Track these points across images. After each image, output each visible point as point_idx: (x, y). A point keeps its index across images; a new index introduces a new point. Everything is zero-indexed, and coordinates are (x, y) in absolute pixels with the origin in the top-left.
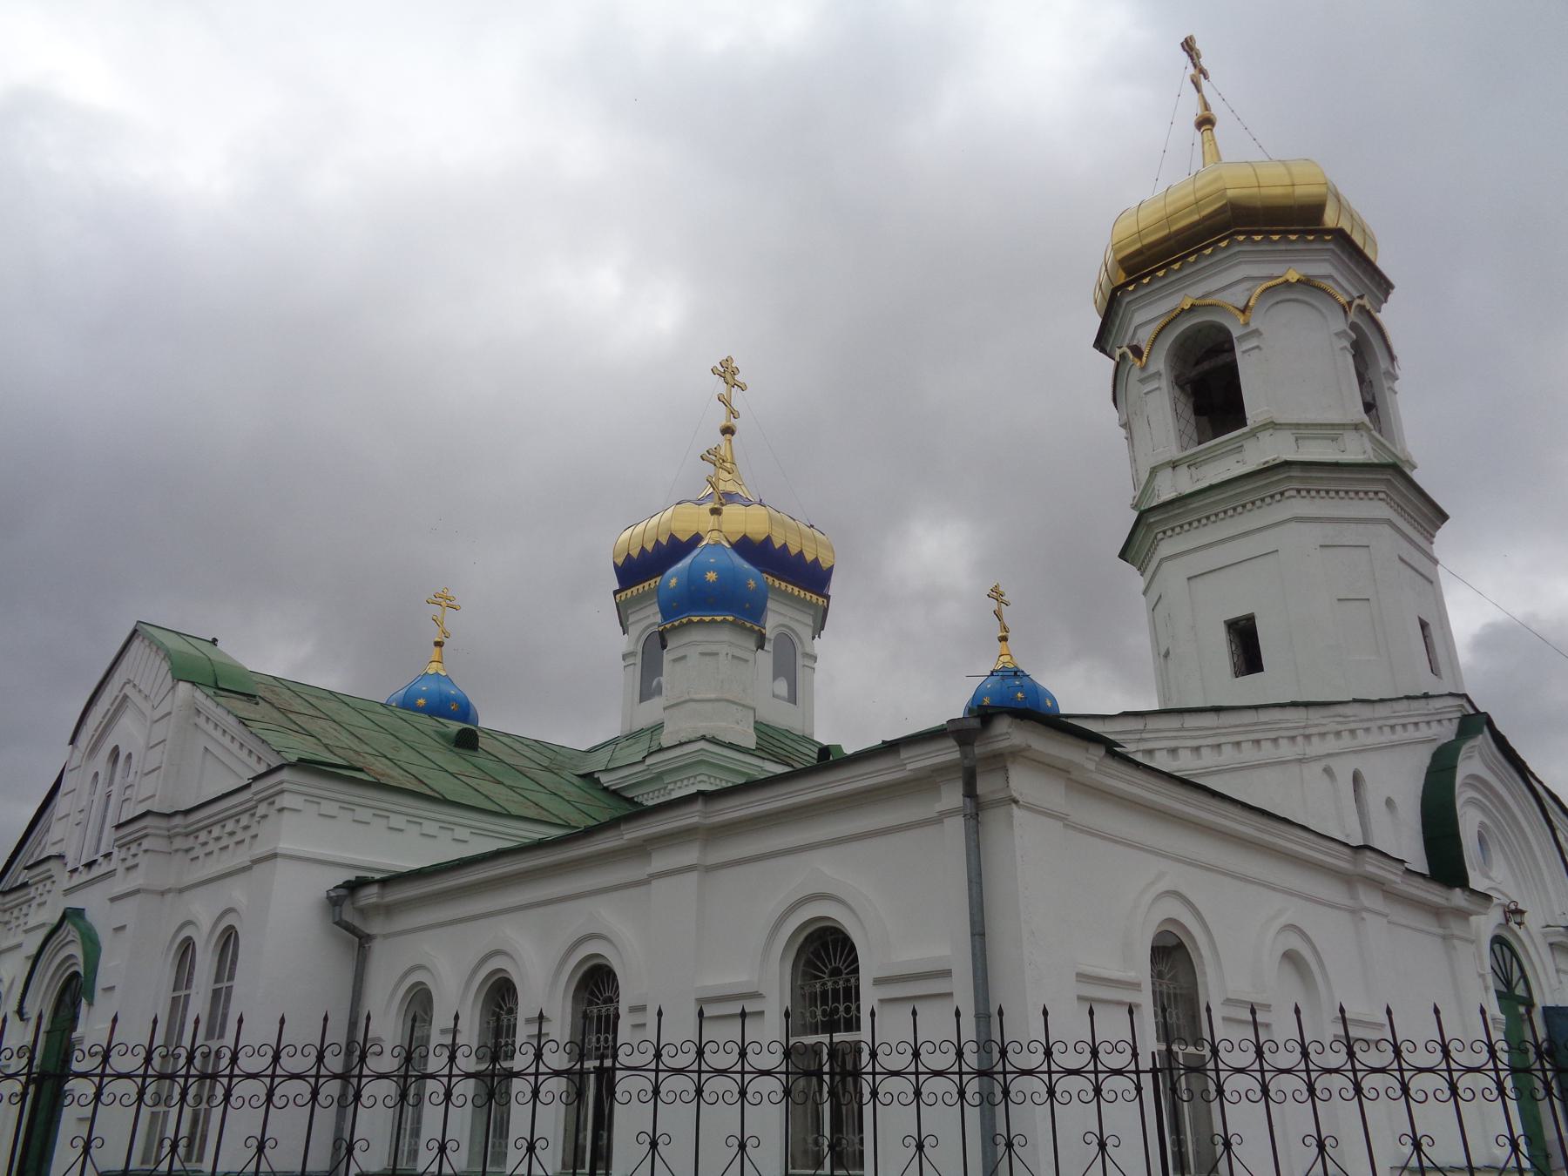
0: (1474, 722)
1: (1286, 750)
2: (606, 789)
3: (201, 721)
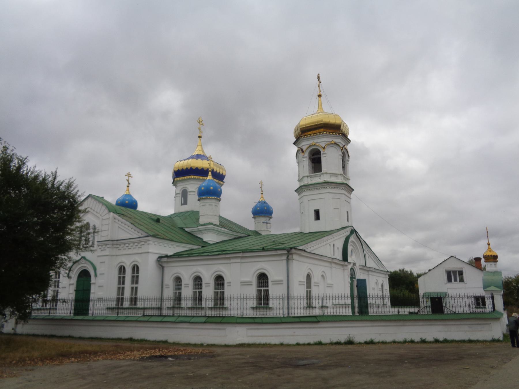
0: (353, 231)
2: (186, 231)
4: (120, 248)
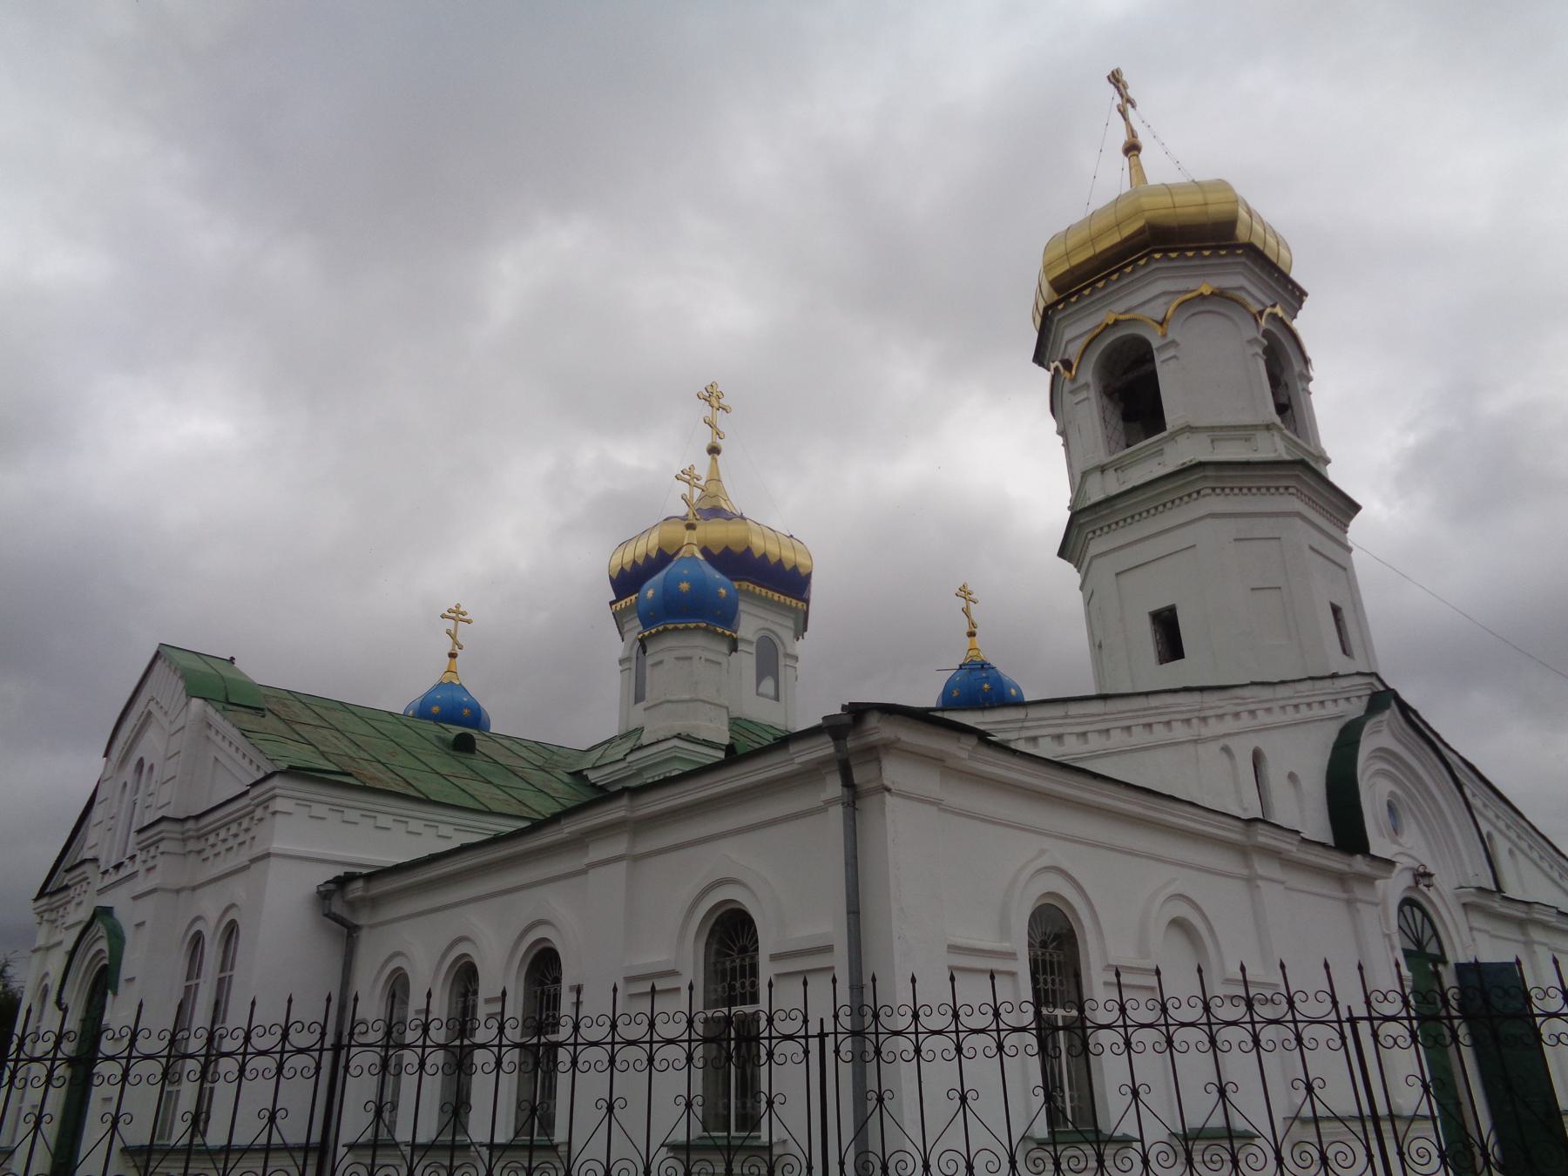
0: (1383, 699)
1: (1180, 732)
2: (594, 785)
3: (212, 734)
4: (209, 853)
